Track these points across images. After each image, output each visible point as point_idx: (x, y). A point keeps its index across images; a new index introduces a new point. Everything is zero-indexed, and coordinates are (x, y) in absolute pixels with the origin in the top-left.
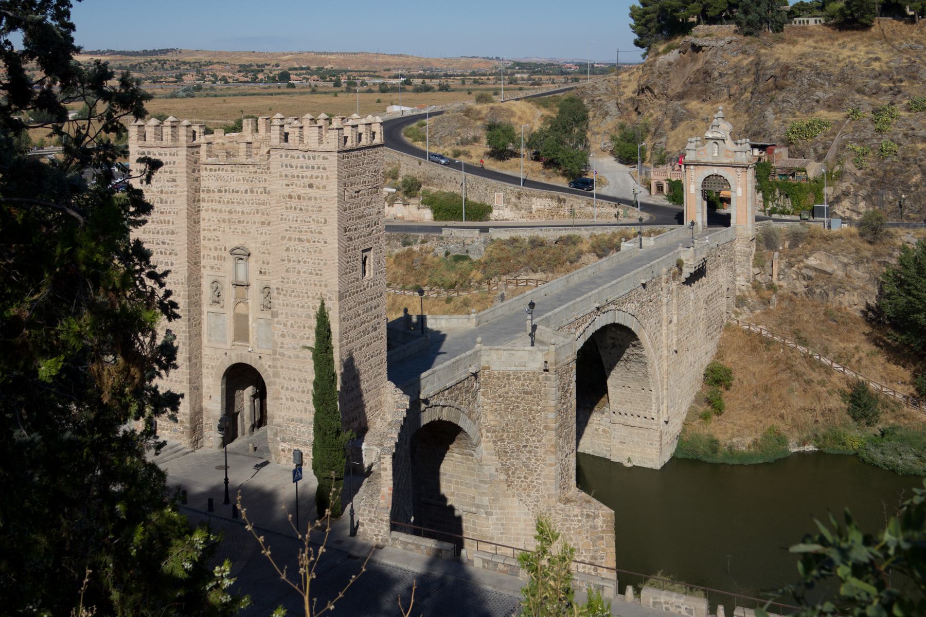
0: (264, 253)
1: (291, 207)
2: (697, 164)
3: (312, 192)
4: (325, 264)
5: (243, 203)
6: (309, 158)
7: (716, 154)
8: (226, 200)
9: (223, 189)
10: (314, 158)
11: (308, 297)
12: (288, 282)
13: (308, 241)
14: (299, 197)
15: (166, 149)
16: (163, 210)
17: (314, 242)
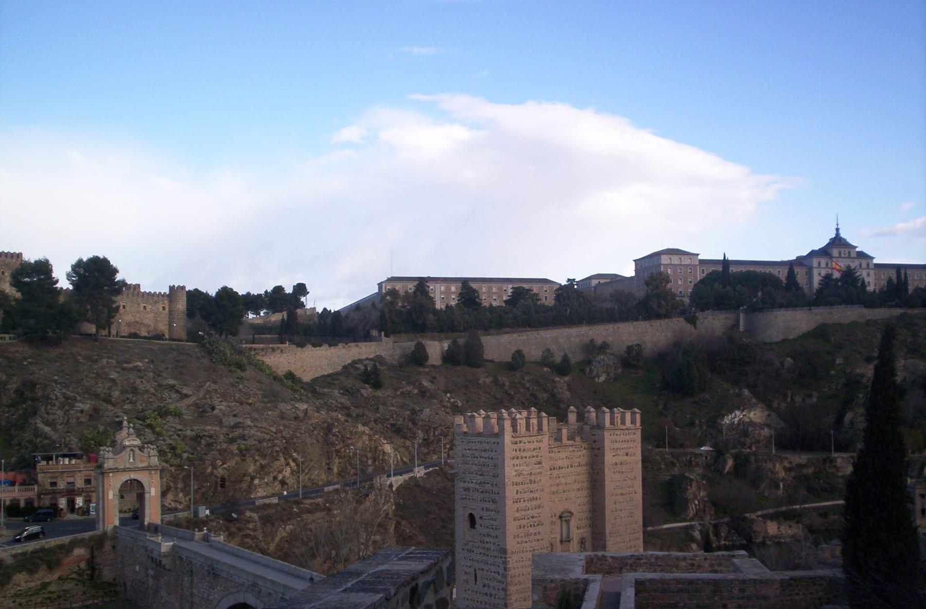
0: (580, 512)
2: (116, 470)
7: (131, 460)
9: (552, 467)
16: (532, 489)
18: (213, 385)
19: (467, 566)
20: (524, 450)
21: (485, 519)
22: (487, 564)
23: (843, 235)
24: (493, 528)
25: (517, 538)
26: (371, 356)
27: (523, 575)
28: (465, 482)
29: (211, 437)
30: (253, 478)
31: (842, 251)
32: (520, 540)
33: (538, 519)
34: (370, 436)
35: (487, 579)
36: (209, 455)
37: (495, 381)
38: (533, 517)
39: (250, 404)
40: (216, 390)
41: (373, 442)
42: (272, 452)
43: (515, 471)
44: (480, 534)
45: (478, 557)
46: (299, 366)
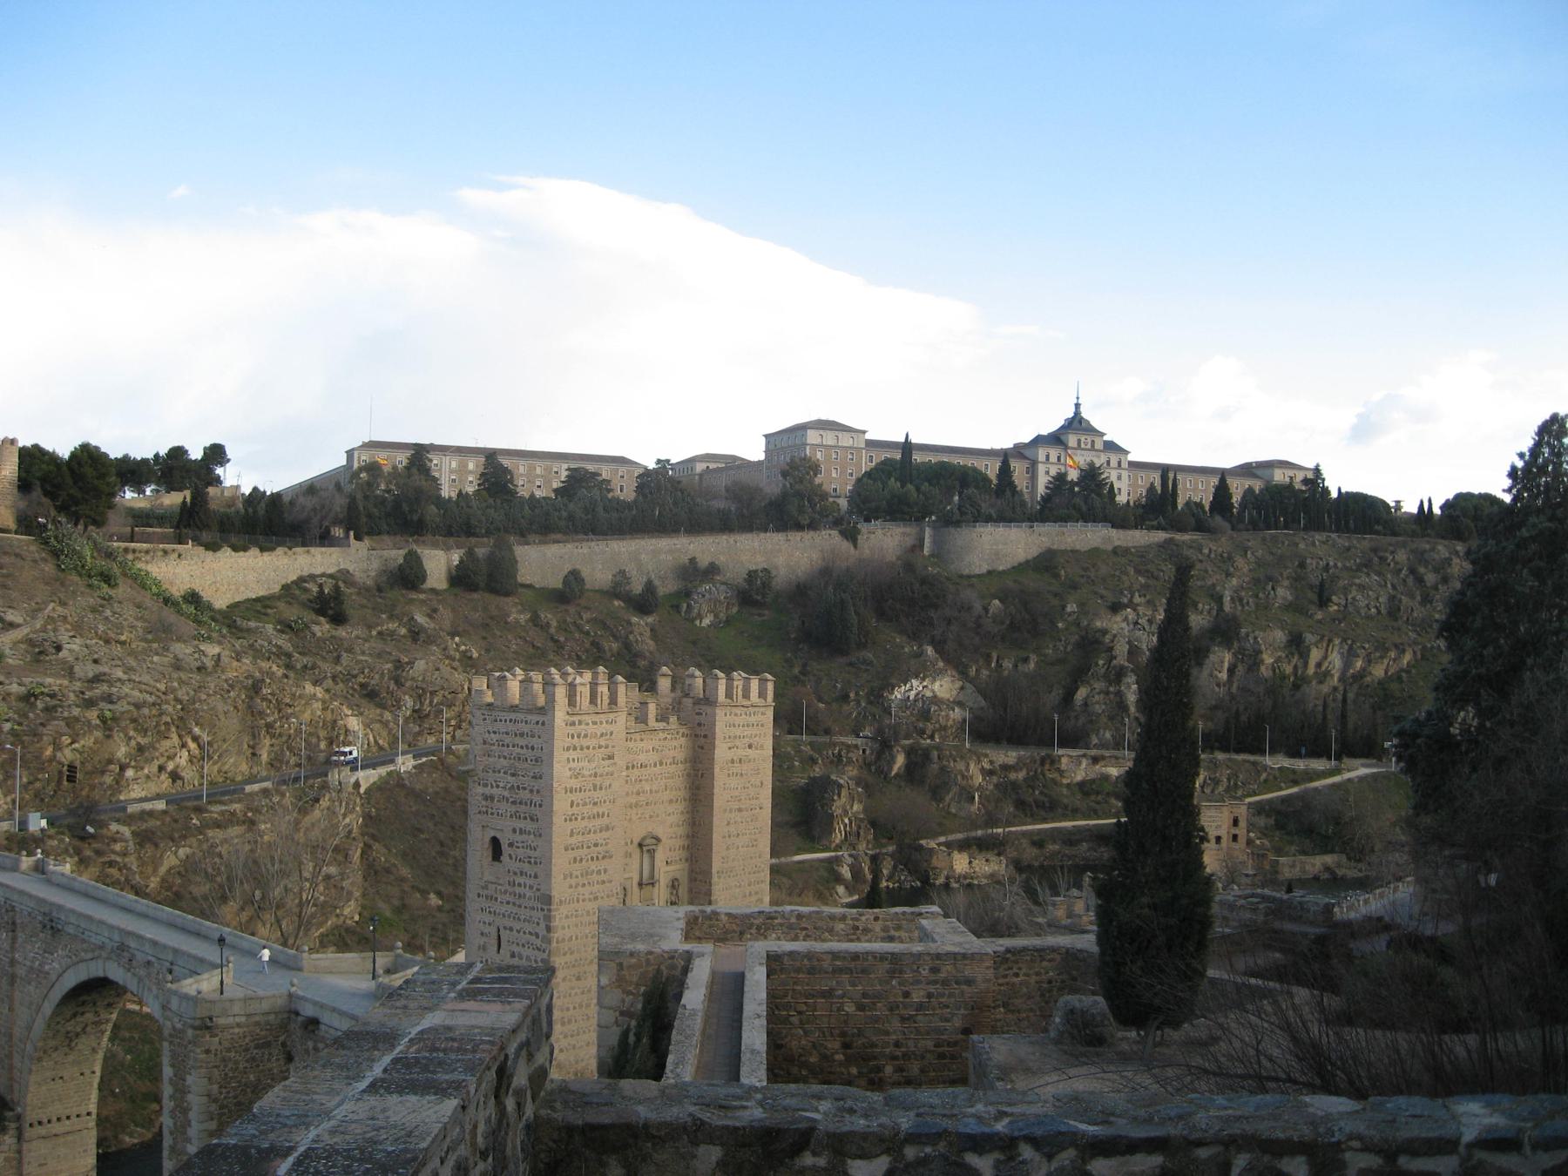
15: (602, 716)
18: (60, 609)
19: (484, 923)
20: (586, 736)
21: (518, 847)
22: (519, 919)
23: (1085, 414)
24: (530, 862)
25: (569, 879)
26: (331, 571)
27: (577, 938)
28: (486, 785)
29: (52, 696)
30: (123, 768)
31: (1083, 439)
32: (573, 882)
33: (605, 848)
34: (324, 702)
35: (518, 944)
36: (49, 727)
37: (535, 620)
38: (596, 845)
39: (123, 643)
40: (65, 618)
41: (329, 711)
42: (158, 724)
44: (509, 871)
45: (503, 908)
46: (209, 582)
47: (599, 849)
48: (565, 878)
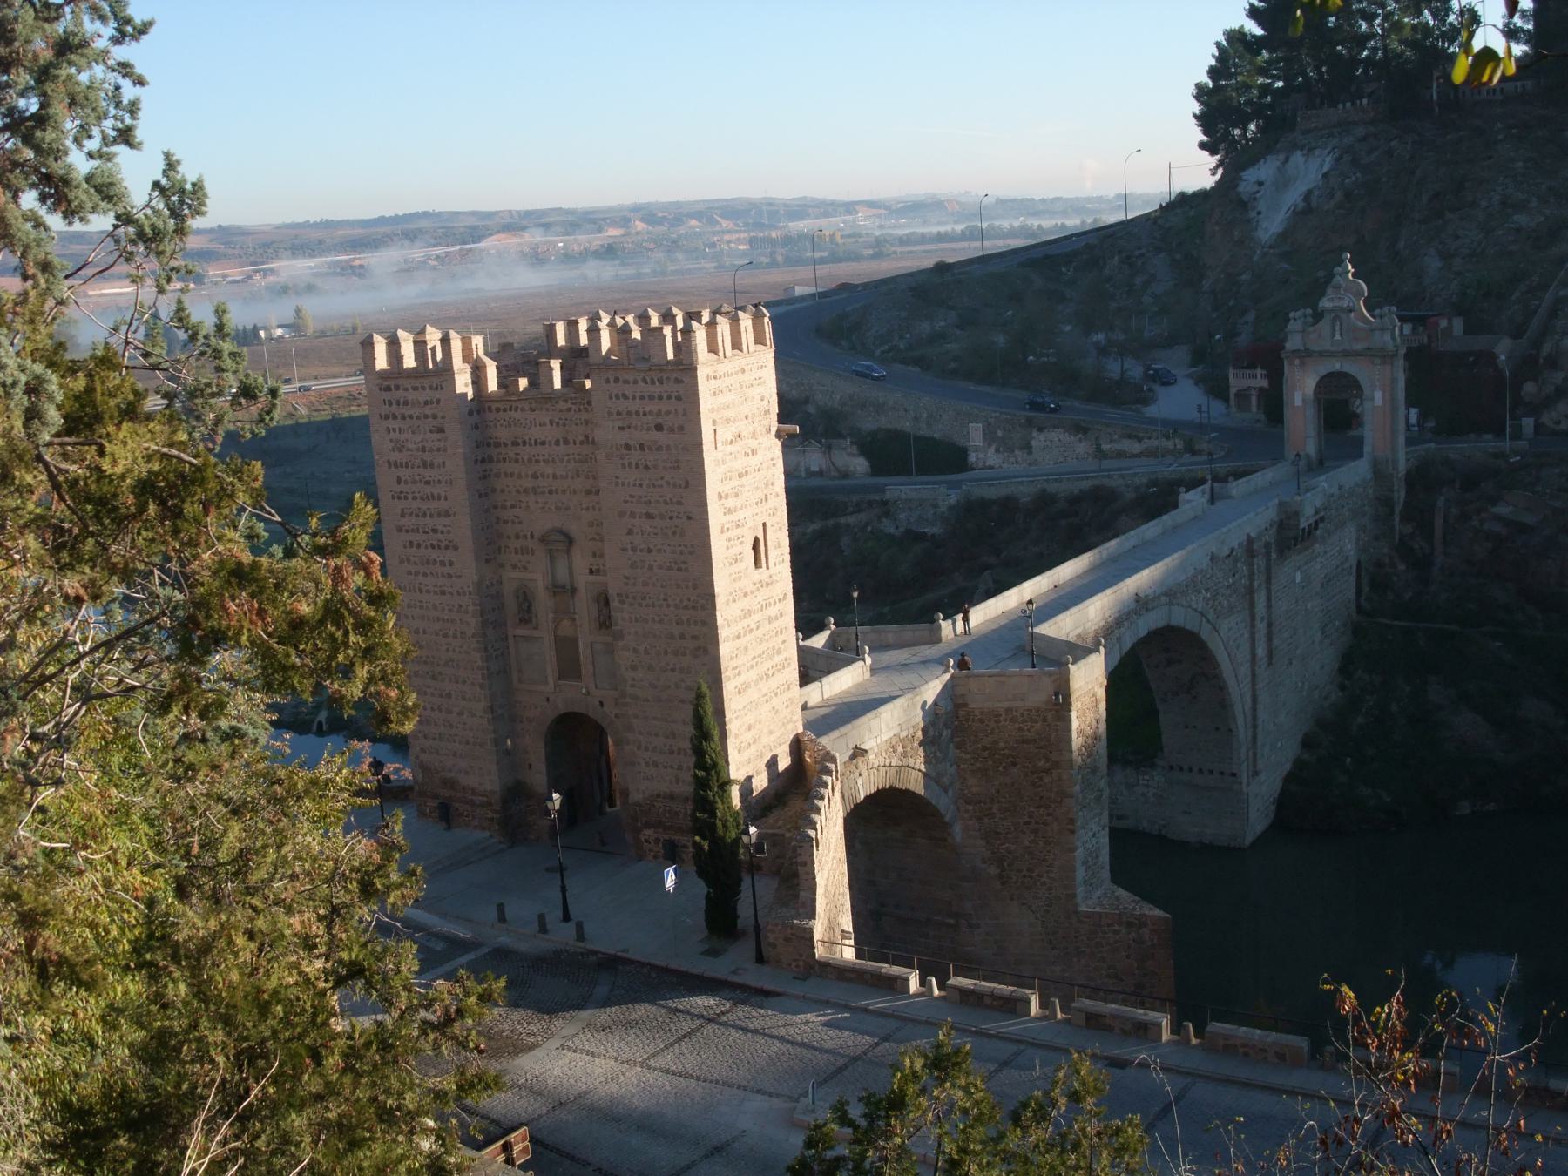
0: (594, 539)
1: (630, 464)
2: (1306, 355)
3: (661, 438)
4: (691, 553)
5: (554, 461)
6: (653, 383)
7: (1338, 337)
8: (526, 458)
10: (661, 382)
11: (668, 606)
12: (634, 584)
13: (662, 517)
14: (642, 447)
17: (671, 518)
20: (406, 403)
38: (434, 531)
43: (391, 441)
47: (439, 536)
48: (402, 562)
